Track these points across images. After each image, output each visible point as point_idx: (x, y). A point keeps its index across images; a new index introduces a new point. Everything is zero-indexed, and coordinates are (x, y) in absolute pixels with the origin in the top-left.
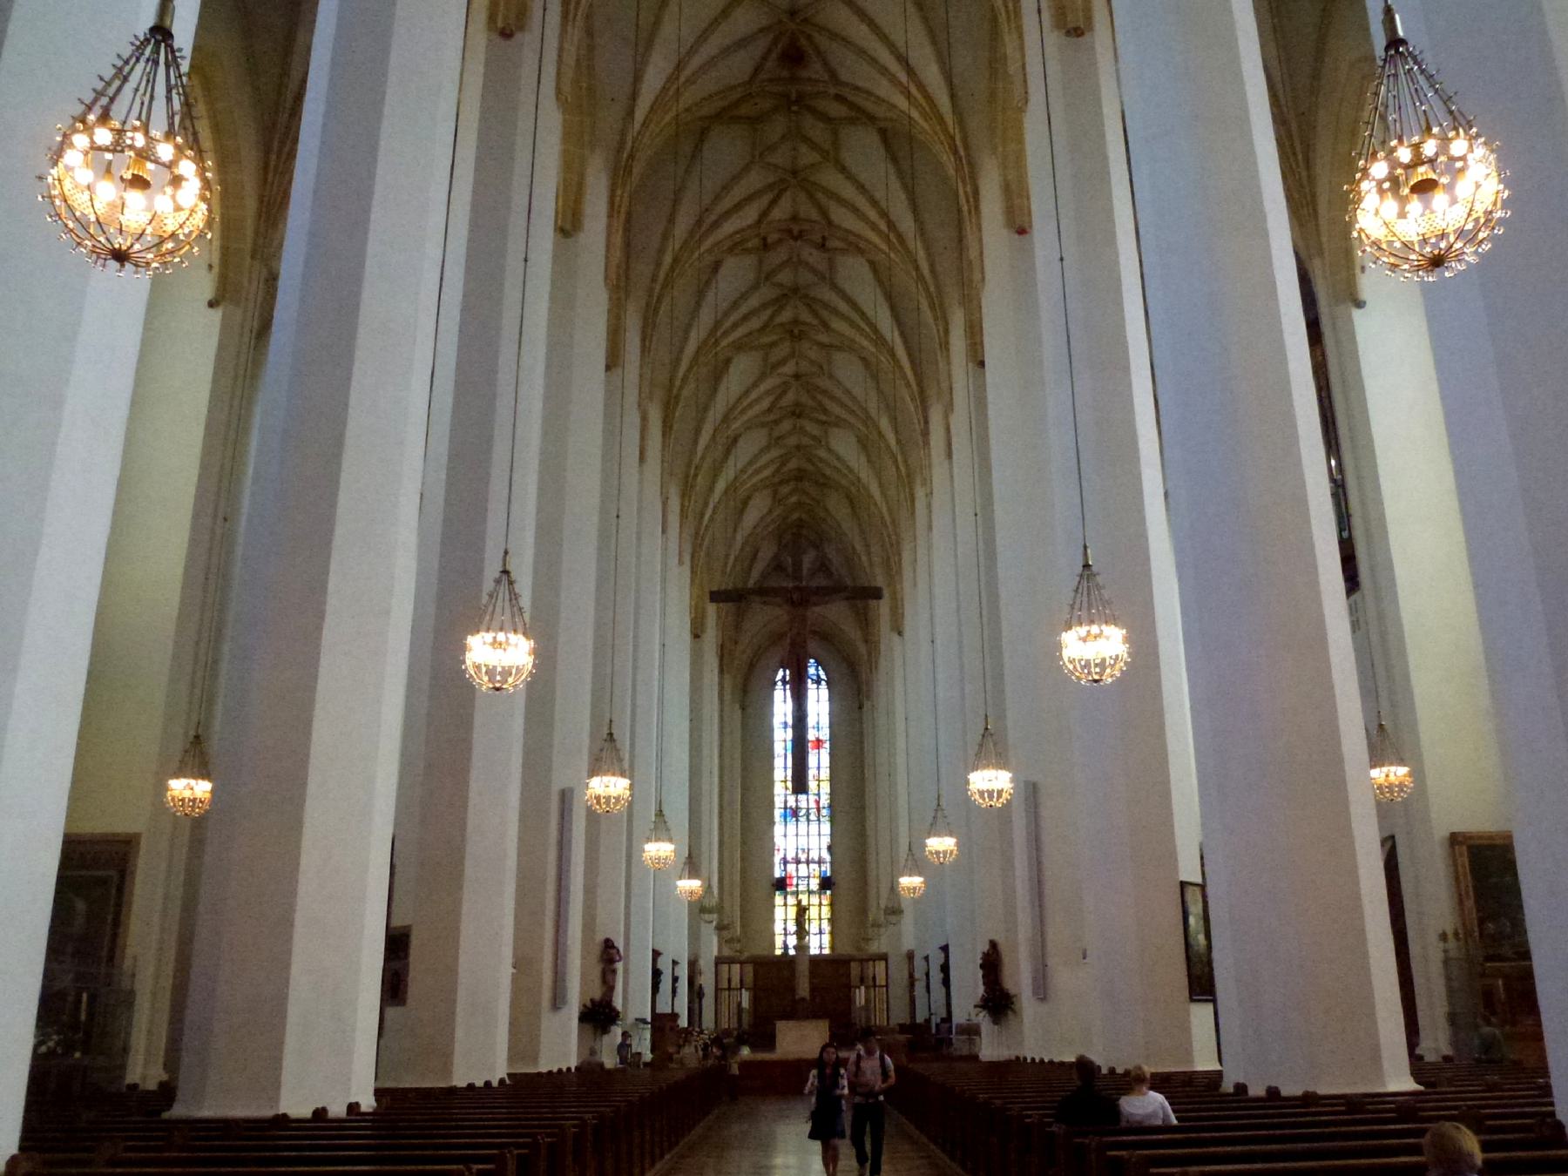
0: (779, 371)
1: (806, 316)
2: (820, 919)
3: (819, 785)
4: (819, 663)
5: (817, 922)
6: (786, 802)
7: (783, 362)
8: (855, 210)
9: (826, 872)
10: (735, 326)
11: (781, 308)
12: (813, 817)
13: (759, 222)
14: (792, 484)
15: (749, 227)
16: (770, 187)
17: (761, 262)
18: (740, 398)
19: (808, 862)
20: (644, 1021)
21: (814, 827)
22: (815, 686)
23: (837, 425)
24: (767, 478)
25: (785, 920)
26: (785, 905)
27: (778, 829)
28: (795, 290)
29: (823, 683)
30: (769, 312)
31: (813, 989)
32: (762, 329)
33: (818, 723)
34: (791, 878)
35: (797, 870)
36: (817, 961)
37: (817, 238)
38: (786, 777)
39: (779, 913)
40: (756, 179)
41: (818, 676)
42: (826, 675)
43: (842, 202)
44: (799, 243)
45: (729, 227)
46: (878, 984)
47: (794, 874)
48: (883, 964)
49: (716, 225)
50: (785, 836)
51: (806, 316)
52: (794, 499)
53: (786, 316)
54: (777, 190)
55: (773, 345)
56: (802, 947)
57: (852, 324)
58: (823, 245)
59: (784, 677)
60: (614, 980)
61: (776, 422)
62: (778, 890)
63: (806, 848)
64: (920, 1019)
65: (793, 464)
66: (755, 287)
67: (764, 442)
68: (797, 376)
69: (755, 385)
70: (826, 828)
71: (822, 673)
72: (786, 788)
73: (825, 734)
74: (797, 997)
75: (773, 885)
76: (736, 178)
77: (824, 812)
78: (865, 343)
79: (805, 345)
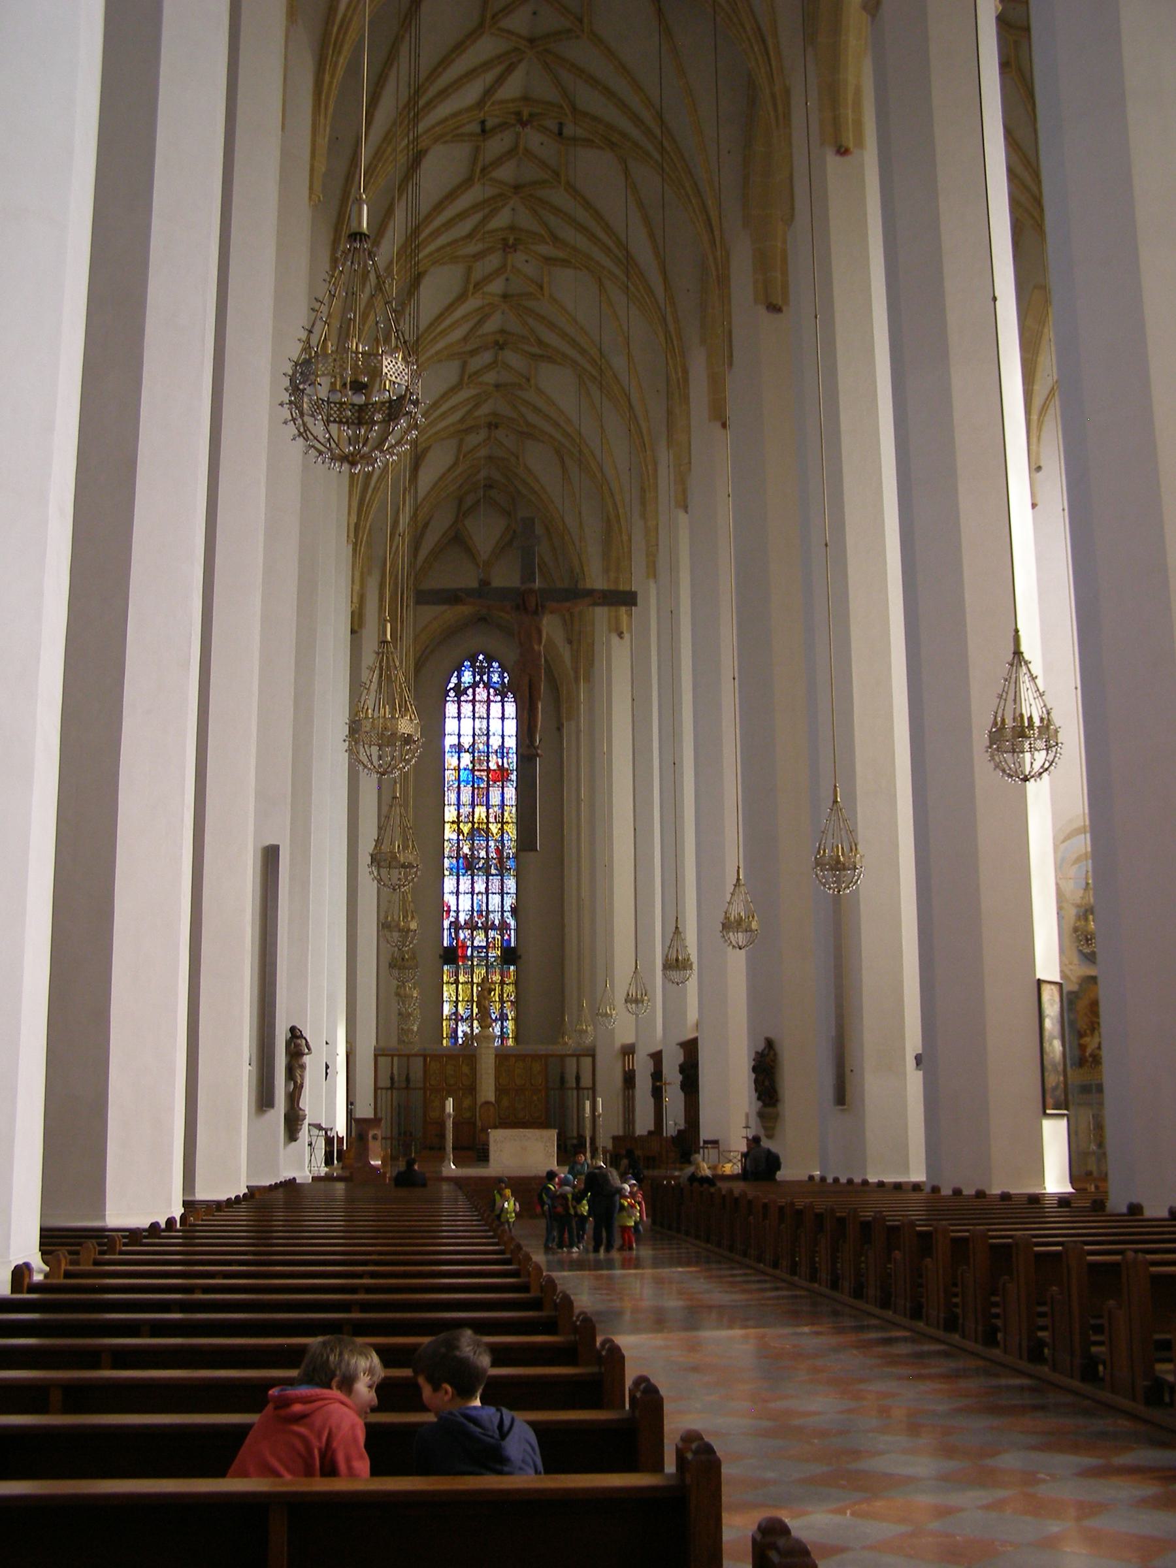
0: (485, 289)
1: (525, 220)
2: (502, 1001)
3: (502, 829)
5: (498, 1005)
6: (459, 849)
7: (488, 279)
8: (609, 93)
9: (509, 940)
10: (436, 233)
11: (494, 212)
12: (493, 871)
13: (480, 104)
14: (483, 434)
15: (469, 109)
16: (499, 58)
17: (477, 149)
18: (431, 324)
19: (486, 928)
20: (319, 1127)
21: (495, 883)
22: (499, 698)
23: (550, 359)
24: (453, 424)
25: (457, 1002)
26: (457, 982)
27: (449, 884)
28: (517, 188)
30: (477, 217)
31: (500, 1090)
32: (470, 236)
33: (502, 746)
35: (472, 939)
36: (502, 1057)
37: (552, 124)
39: (448, 992)
40: (486, 47)
43: (593, 81)
44: (528, 129)
45: (443, 110)
47: (469, 943)
48: (589, 1060)
49: (430, 105)
50: (457, 893)
51: (525, 220)
52: (483, 452)
53: (501, 220)
54: (508, 63)
55: (478, 256)
56: (484, 1038)
57: (592, 237)
58: (560, 134)
59: (458, 685)
60: (302, 1077)
61: (473, 353)
63: (484, 908)
64: (644, 1124)
65: (484, 410)
66: (467, 183)
67: (453, 379)
68: (505, 296)
69: (450, 308)
70: (511, 884)
72: (460, 832)
74: (481, 1099)
75: (441, 957)
76: (459, 47)
77: (510, 864)
78: (606, 262)
79: (518, 259)
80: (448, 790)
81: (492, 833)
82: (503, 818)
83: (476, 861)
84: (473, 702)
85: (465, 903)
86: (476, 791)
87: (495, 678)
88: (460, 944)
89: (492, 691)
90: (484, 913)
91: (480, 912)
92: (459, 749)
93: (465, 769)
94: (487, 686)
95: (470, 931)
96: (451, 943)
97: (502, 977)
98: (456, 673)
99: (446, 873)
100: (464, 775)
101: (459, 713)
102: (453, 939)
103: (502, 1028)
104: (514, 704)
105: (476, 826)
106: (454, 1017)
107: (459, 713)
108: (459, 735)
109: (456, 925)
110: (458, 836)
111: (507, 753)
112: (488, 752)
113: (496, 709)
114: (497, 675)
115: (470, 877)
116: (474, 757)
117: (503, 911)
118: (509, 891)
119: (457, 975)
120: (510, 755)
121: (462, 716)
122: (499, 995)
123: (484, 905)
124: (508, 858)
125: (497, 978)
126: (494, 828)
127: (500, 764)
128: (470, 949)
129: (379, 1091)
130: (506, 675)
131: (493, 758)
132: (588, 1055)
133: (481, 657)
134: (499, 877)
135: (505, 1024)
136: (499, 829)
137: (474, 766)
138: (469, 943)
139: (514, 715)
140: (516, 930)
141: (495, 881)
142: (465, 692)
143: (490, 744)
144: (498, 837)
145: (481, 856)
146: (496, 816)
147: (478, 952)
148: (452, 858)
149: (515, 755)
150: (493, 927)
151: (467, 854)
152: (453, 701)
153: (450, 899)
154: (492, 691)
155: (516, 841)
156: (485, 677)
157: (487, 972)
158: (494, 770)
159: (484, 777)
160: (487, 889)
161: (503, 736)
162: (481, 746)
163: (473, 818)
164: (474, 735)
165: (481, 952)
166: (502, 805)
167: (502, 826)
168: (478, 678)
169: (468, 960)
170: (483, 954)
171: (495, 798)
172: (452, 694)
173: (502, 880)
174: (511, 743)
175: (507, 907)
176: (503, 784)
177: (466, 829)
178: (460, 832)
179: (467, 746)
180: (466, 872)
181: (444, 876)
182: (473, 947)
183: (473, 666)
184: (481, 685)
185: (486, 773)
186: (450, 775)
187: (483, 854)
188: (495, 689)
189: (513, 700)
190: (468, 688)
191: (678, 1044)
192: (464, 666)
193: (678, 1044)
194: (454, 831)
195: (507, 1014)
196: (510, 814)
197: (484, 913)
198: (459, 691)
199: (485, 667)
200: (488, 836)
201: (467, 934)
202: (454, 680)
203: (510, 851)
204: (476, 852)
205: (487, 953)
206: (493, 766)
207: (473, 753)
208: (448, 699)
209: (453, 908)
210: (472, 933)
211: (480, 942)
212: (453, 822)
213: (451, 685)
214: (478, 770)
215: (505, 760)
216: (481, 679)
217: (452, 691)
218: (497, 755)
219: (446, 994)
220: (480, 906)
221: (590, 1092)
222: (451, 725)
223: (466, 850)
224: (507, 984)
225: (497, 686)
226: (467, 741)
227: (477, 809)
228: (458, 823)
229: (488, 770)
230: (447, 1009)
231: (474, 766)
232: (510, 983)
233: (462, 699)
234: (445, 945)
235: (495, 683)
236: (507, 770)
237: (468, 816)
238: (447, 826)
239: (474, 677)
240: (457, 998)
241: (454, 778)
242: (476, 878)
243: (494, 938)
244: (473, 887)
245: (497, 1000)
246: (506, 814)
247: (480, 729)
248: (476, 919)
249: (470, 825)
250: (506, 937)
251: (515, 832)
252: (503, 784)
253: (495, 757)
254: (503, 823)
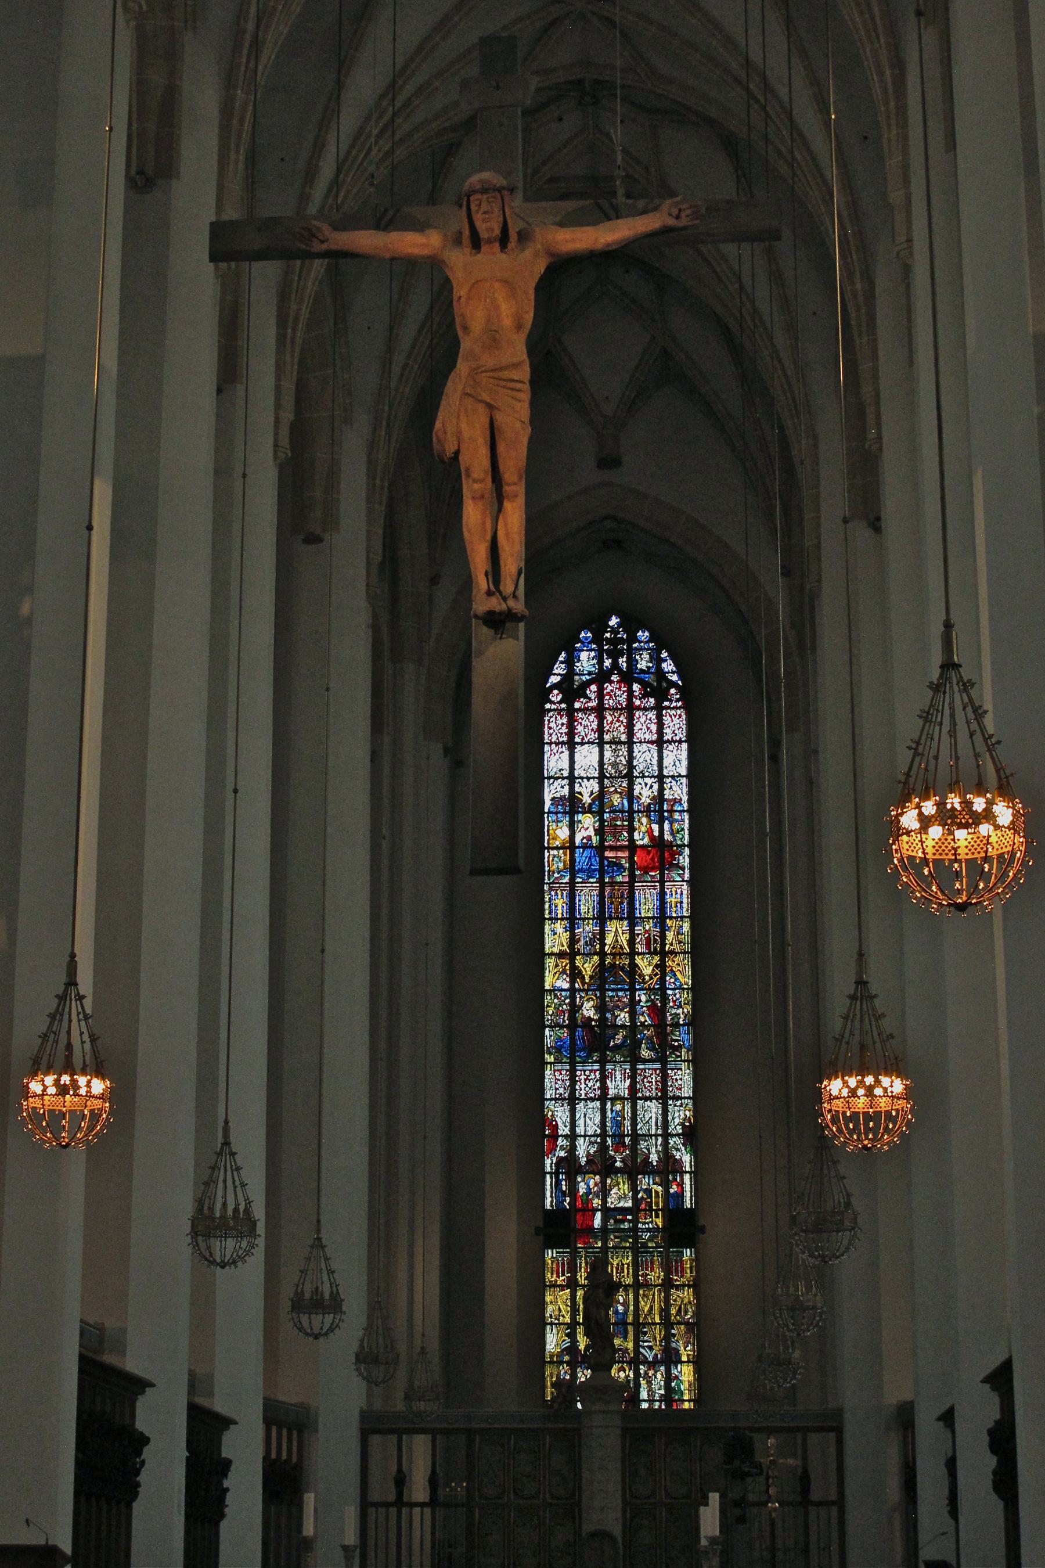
2: (667, 1324)
4: (660, 641)
5: (658, 1332)
6: (574, 1009)
9: (680, 1195)
12: (645, 1053)
27: (554, 1081)
29: (673, 691)
35: (605, 1193)
38: (573, 940)
41: (661, 674)
42: (679, 672)
46: (816, 1495)
47: (597, 1202)
50: (572, 1101)
62: (551, 1243)
70: (683, 1079)
71: (668, 666)
72: (575, 974)
74: (588, 1527)
75: (538, 1231)
77: (682, 1037)
80: (551, 889)
81: (642, 975)
82: (663, 944)
83: (610, 1032)
84: (600, 711)
85: (589, 1119)
86: (608, 890)
87: (643, 663)
88: (579, 1204)
89: (636, 687)
90: (627, 1140)
91: (619, 1137)
92: (572, 805)
93: (584, 847)
94: (628, 678)
95: (598, 1177)
96: (560, 1203)
97: (667, 1269)
98: (563, 656)
99: (550, 1058)
100: (582, 858)
101: (571, 733)
102: (564, 1193)
103: (668, 1378)
104: (681, 712)
105: (608, 961)
106: (566, 1358)
107: (571, 733)
108: (572, 779)
109: (570, 1166)
110: (572, 982)
111: (671, 811)
112: (631, 811)
113: (644, 725)
114: (646, 656)
115: (596, 1067)
116: (602, 821)
117: (666, 1136)
118: (678, 1093)
119: (573, 1269)
120: (677, 816)
121: (577, 739)
122: (661, 1310)
123: (627, 1123)
124: (676, 1025)
125: (656, 1275)
126: (646, 966)
127: (656, 834)
128: (598, 1215)
129: (372, 1511)
130: (664, 654)
131: (642, 823)
132: (831, 1429)
133: (614, 621)
134: (658, 1066)
135: (674, 1372)
136: (656, 966)
137: (602, 840)
138: (597, 1202)
139: (681, 735)
140: (695, 1174)
141: (648, 1073)
142: (581, 692)
143: (636, 793)
144: (654, 983)
145: (619, 1023)
146: (648, 940)
147: (617, 1221)
148: (561, 1027)
149: (686, 816)
150: (646, 1168)
151: (590, 1019)
152: (559, 711)
153: (560, 1114)
154: (636, 687)
155: (694, 989)
156: (623, 662)
157: (636, 1265)
158: (643, 847)
159: (623, 861)
160: (632, 1089)
161: (661, 778)
162: (616, 800)
163: (603, 945)
164: (601, 777)
165: (622, 1221)
166: (661, 918)
167: (662, 959)
168: (607, 663)
169: (596, 1238)
170: (626, 1225)
172: (556, 696)
173: (664, 1072)
174: (679, 791)
175: (676, 1128)
176: (662, 875)
177: (588, 967)
178: (575, 974)
179: (587, 799)
180: (589, 1056)
181: (544, 1064)
182: (607, 1212)
183: (598, 639)
184: (615, 678)
185: (627, 854)
186: (555, 861)
187: (623, 1017)
188: (644, 684)
189: (679, 704)
190: (587, 684)
191: (983, 1381)
192: (579, 641)
193: (983, 1381)
194: (564, 972)
195: (677, 1351)
197: (627, 1140)
198: (571, 690)
199: (622, 641)
200: (633, 982)
201: (592, 1183)
202: (559, 669)
203: (680, 1011)
204: (608, 1015)
205: (635, 1221)
206: (641, 838)
207: (600, 813)
208: (548, 706)
209: (564, 1130)
210: (603, 1182)
211: (620, 1199)
212: (561, 955)
213: (554, 679)
214: (612, 848)
215: (666, 826)
216: (615, 665)
217: (556, 692)
218: (648, 816)
219: (550, 1309)
220: (619, 1125)
221: (834, 1511)
222: (555, 761)
223: (588, 1010)
224: (678, 1288)
225: (647, 678)
226: (587, 790)
227: (611, 926)
228: (571, 954)
229: (632, 847)
230: (553, 1341)
231: (602, 840)
232: (684, 1285)
233: (577, 705)
234: (548, 1207)
235: (642, 671)
236: (670, 845)
237: (592, 941)
238: (550, 962)
239: (601, 662)
240: (573, 1317)
241: (561, 865)
242: (609, 1067)
243: (648, 1191)
244: (604, 1088)
245: (657, 1320)
246: (670, 936)
247: (615, 765)
248: (612, 1153)
249: (596, 958)
250: (674, 1189)
251: (689, 972)
252: (662, 875)
253: (644, 820)
254: (663, 954)
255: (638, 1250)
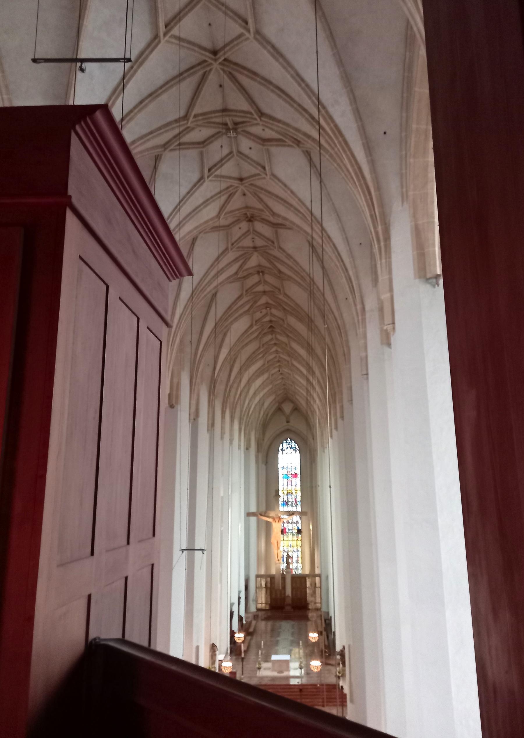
12: (293, 505)
34: (285, 529)
71: (297, 447)
73: (298, 472)
87: (293, 446)
97: (297, 537)
124: (298, 501)
126: (294, 492)
130: (296, 445)
133: (289, 439)
156: (290, 446)
171: (294, 484)
177: (286, 492)
183: (287, 442)
184: (289, 448)
196: (299, 488)
198: (282, 450)
229: (292, 474)
255: (293, 535)
